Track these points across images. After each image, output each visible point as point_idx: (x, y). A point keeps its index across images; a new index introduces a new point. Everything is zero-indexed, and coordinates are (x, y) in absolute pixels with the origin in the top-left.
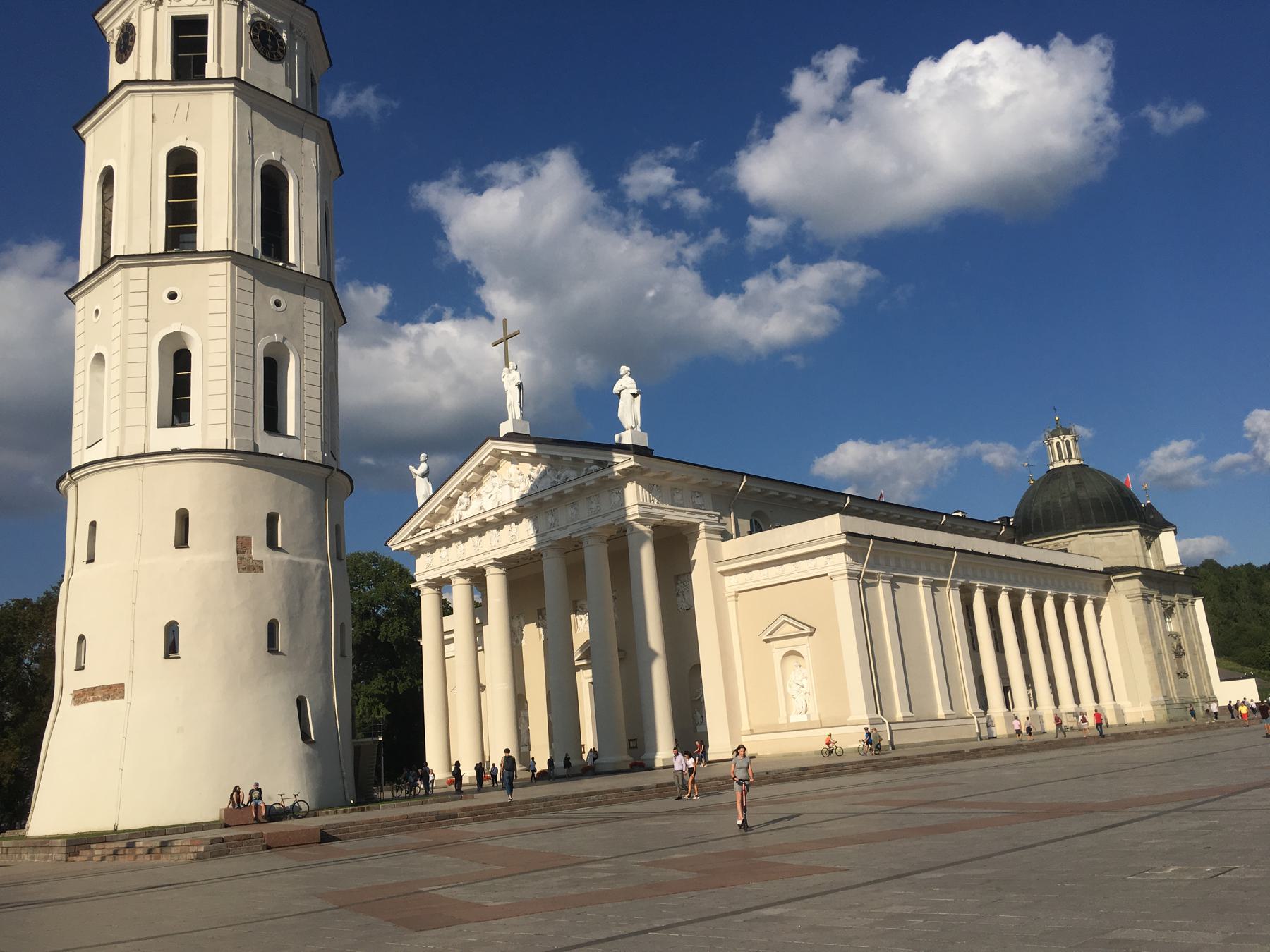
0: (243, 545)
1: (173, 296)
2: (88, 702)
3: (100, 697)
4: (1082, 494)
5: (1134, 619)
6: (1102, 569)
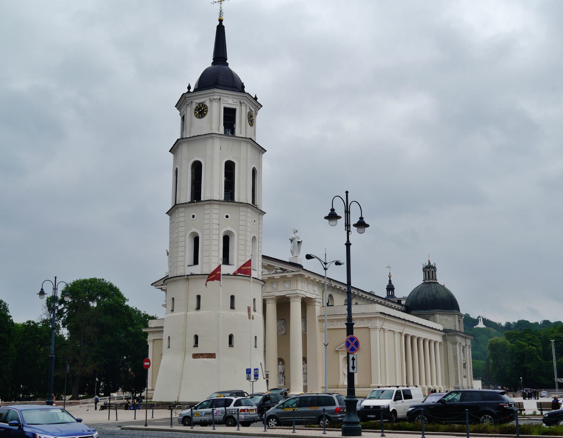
0: (249, 309)
1: (227, 217)
2: (200, 358)
3: (205, 357)
4: (437, 296)
5: (452, 352)
6: (442, 330)
